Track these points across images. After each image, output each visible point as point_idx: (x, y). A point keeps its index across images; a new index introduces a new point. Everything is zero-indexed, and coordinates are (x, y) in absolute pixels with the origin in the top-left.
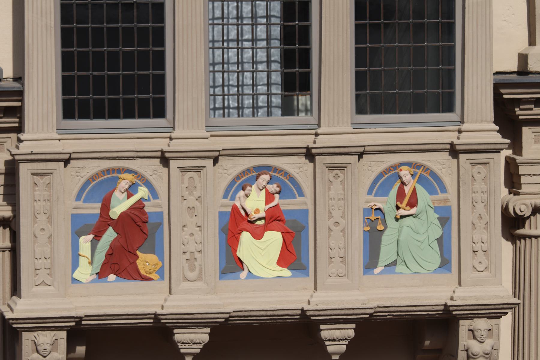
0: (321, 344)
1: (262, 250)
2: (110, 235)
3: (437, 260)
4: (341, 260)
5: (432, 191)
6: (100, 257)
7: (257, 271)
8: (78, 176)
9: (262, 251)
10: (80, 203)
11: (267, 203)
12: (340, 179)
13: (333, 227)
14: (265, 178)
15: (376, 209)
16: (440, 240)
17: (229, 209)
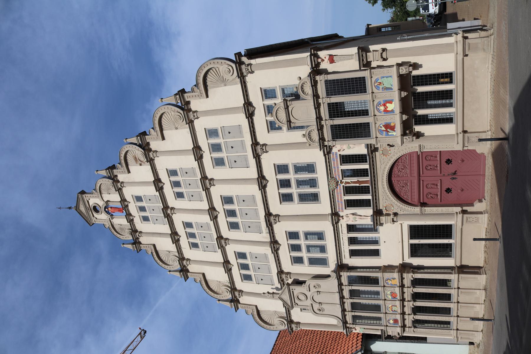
0: (405, 96)
2: (388, 130)
3: (390, 78)
5: (379, 79)
6: (392, 131)
7: (394, 107)
10: (384, 135)
11: (382, 106)
14: (378, 107)
16: (387, 78)
17: (383, 112)
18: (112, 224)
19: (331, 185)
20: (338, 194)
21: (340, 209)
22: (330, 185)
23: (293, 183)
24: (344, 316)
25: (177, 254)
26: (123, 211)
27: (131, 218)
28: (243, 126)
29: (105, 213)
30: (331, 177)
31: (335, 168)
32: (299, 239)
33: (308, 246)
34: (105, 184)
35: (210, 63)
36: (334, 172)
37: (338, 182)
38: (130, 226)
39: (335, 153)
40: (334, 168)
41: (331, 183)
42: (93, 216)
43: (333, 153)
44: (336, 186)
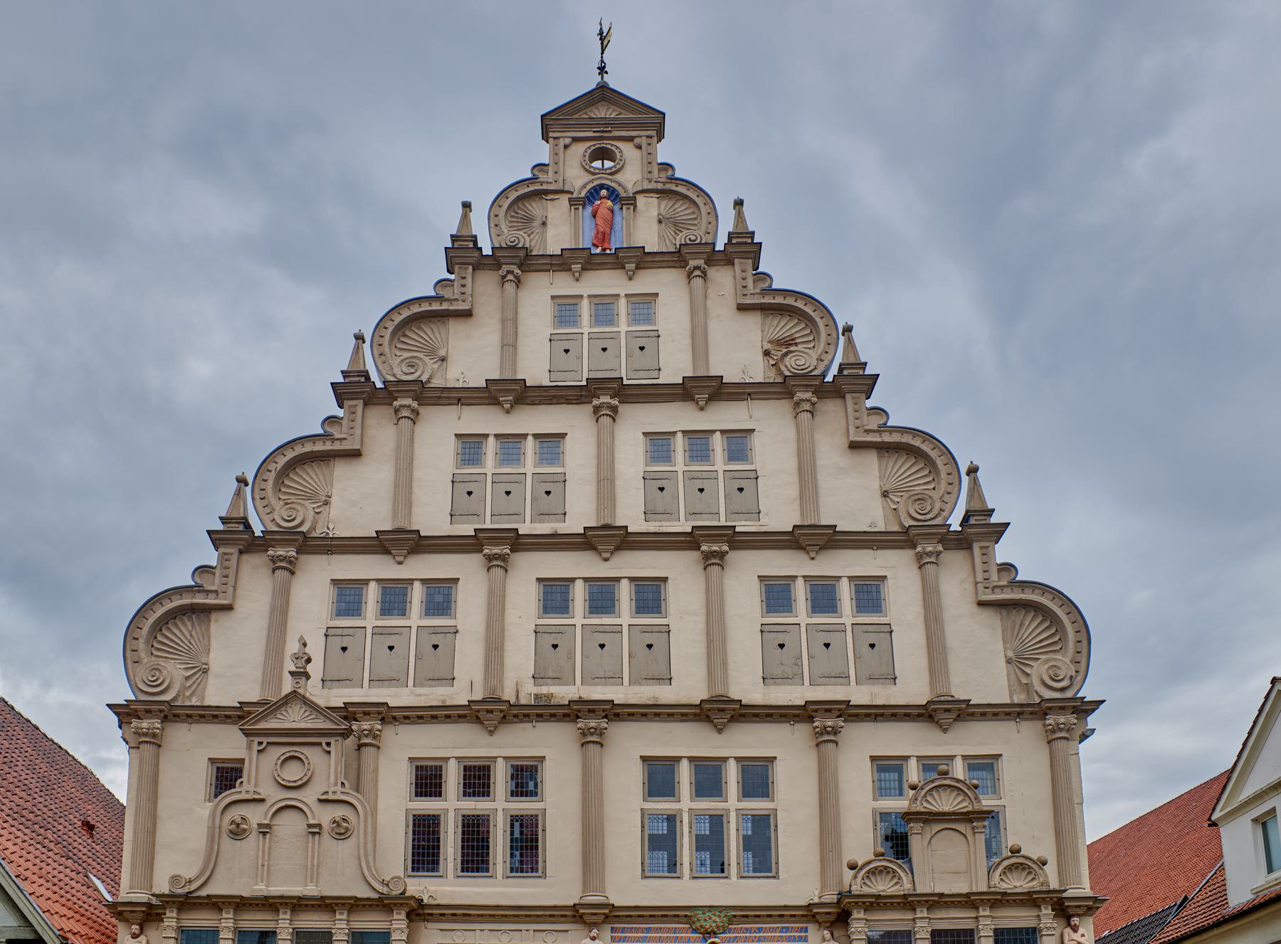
18: (547, 192)
19: (708, 914)
20: (675, 931)
21: (624, 933)
22: (710, 911)
23: (709, 805)
24: (216, 904)
25: (437, 383)
26: (600, 248)
27: (576, 267)
28: (891, 689)
29: (591, 185)
30: (734, 916)
31: (759, 932)
32: (512, 795)
33: (488, 820)
34: (695, 219)
35: (1079, 632)
36: (746, 929)
37: (715, 937)
38: (540, 253)
39: (806, 936)
40: (760, 930)
41: (715, 915)
42: (575, 140)
43: (806, 930)
44: (702, 930)
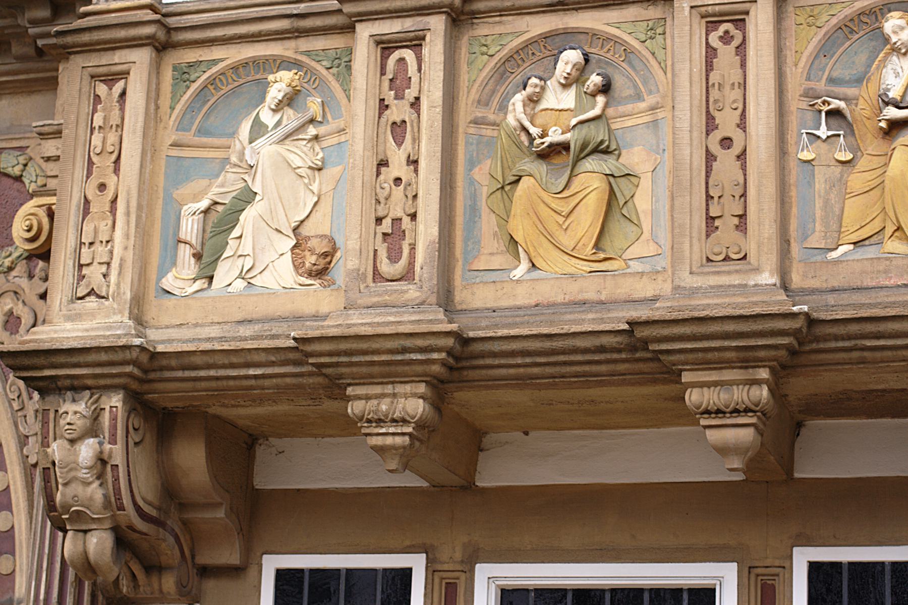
1: (563, 216)
4: (737, 223)
8: (185, 82)
9: (564, 219)
12: (736, 42)
13: (715, 148)
14: (571, 57)
15: (829, 113)
